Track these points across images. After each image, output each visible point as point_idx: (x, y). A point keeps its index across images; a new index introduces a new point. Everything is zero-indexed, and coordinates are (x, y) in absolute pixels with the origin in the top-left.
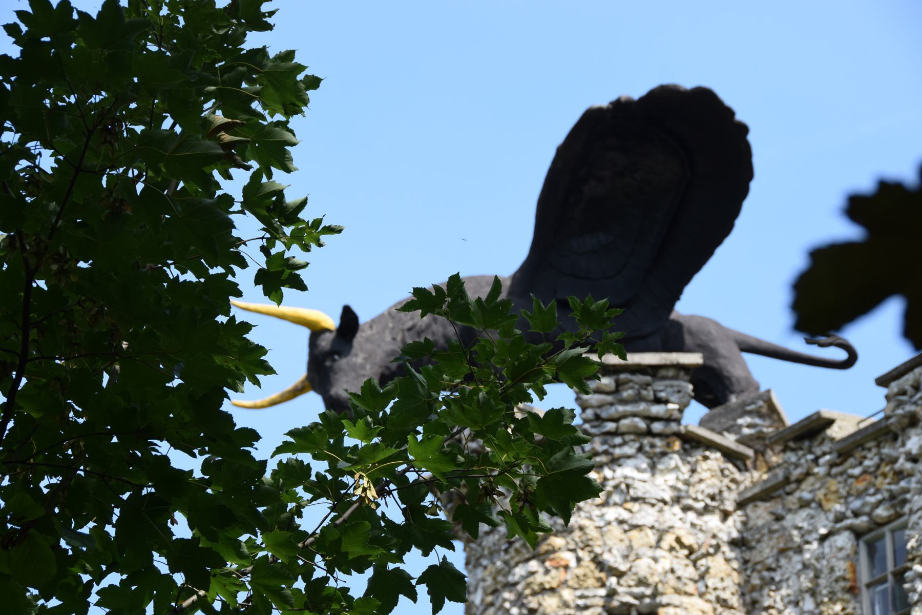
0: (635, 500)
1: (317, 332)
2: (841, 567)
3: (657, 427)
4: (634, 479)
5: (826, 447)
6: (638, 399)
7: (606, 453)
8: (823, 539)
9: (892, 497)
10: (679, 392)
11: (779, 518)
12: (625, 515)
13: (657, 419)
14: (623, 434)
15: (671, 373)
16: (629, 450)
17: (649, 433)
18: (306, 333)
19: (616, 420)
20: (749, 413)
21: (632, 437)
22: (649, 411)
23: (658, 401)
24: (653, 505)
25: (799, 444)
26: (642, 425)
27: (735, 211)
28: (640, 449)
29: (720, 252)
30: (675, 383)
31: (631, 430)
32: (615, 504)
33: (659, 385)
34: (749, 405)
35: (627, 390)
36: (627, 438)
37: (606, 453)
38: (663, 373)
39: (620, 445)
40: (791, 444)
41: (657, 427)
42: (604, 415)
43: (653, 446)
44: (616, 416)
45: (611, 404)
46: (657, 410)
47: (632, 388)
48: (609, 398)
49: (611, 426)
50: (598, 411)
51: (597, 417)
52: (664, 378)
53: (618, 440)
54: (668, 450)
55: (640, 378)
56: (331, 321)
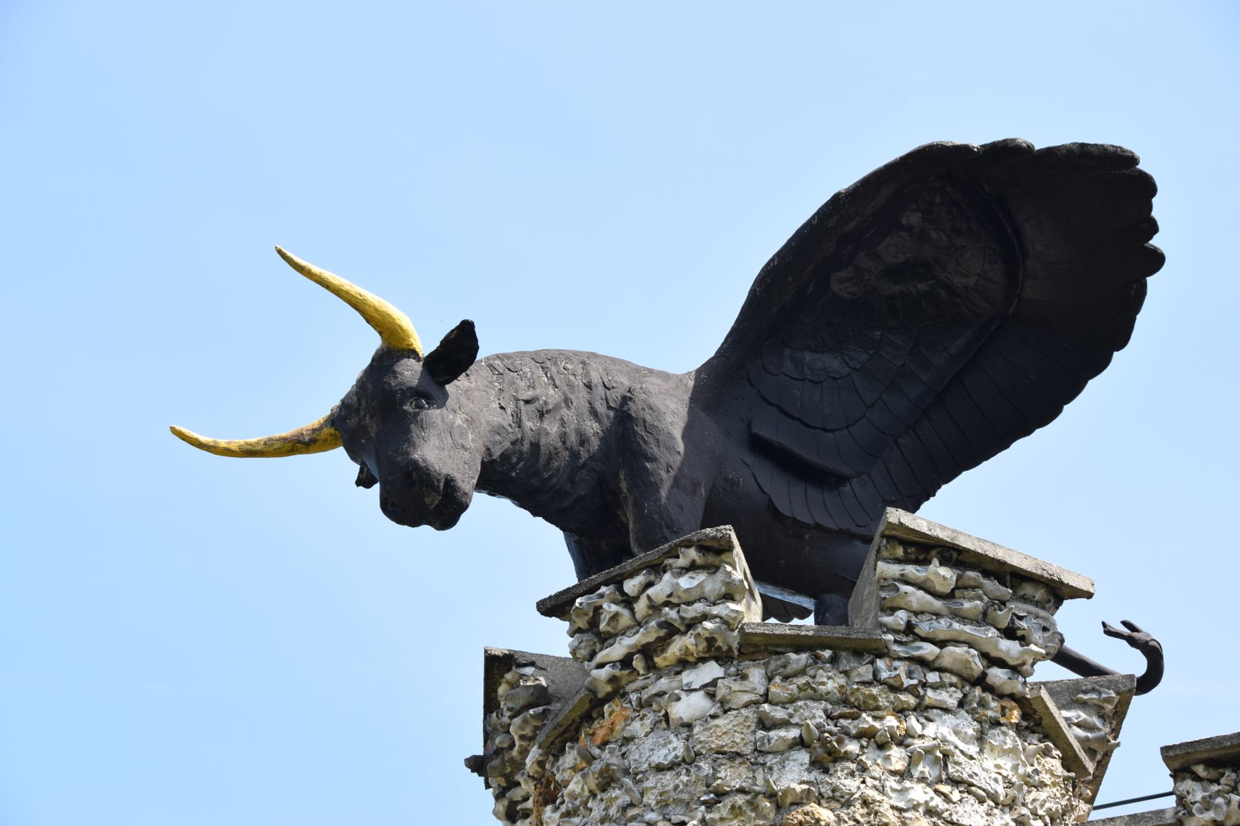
0: (955, 782)
1: (394, 348)
3: (998, 675)
4: (956, 747)
6: (984, 619)
7: (911, 690)
10: (1045, 629)
12: (938, 802)
13: (1001, 663)
14: (941, 670)
15: (1039, 594)
16: (950, 698)
17: (981, 681)
18: (372, 342)
19: (942, 644)
20: (1083, 705)
21: (954, 679)
22: (996, 646)
23: (1009, 633)
24: (981, 801)
25: (1213, 774)
26: (978, 665)
27: (1072, 390)
28: (961, 704)
29: (1019, 445)
30: (1042, 613)
31: (955, 668)
32: (922, 779)
34: (1085, 692)
35: (971, 599)
36: (949, 678)
37: (911, 690)
38: (1028, 590)
39: (935, 687)
40: (1200, 770)
41: (998, 675)
42: (924, 627)
43: (983, 704)
44: (941, 636)
45: (938, 615)
46: (1009, 648)
47: (981, 599)
48: (938, 604)
49: (928, 650)
50: (914, 620)
51: (909, 629)
52: (1024, 599)
53: (933, 677)
54: (1002, 720)
55: (992, 585)
56: (426, 341)
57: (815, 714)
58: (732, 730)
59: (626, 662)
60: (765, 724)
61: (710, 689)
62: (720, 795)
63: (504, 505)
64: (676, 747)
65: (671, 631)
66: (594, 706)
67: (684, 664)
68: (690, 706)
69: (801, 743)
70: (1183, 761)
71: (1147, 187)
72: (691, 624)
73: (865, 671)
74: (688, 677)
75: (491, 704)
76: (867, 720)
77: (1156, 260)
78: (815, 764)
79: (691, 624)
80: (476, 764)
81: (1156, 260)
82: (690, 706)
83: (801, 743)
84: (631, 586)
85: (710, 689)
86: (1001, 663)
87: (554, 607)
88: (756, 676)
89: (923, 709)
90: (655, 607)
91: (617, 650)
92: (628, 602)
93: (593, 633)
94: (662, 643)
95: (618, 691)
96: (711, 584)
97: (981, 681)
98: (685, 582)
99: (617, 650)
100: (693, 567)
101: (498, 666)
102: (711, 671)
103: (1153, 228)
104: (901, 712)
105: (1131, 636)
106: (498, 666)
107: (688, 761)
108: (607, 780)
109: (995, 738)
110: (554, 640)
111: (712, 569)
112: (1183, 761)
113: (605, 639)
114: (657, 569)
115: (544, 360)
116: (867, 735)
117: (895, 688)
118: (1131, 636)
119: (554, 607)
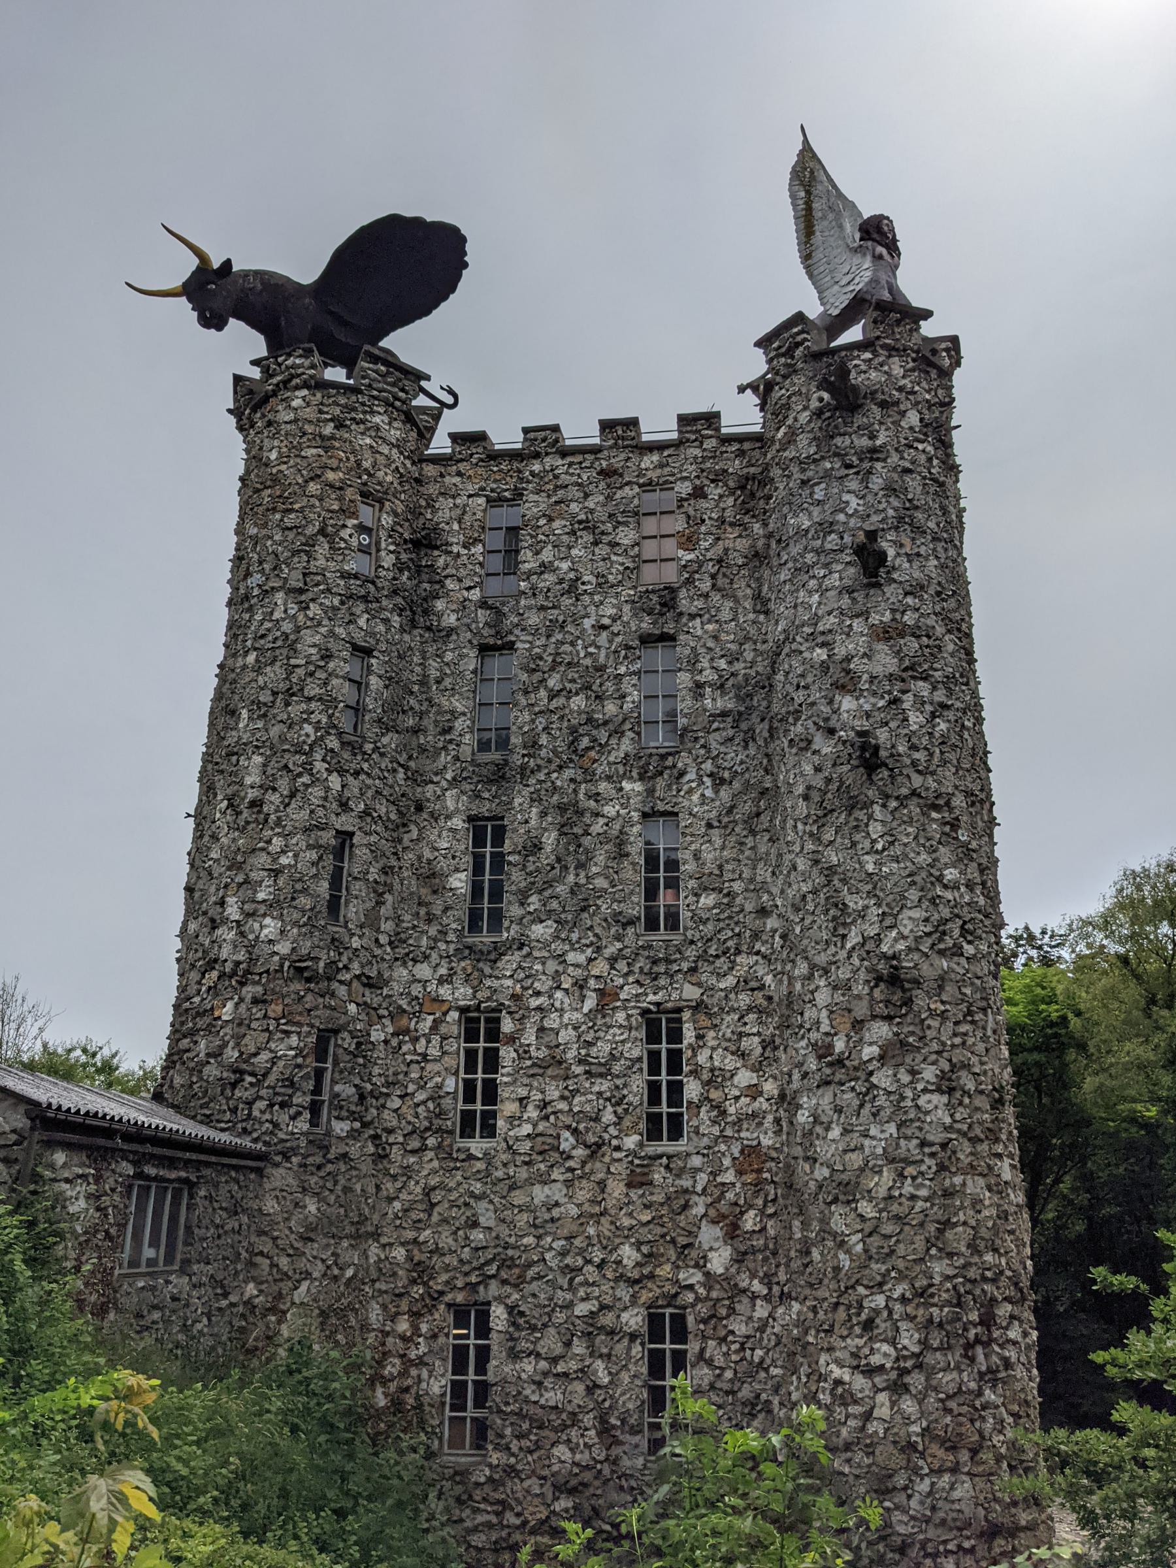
2: (479, 515)
3: (398, 404)
5: (480, 450)
6: (394, 385)
8: (470, 496)
9: (516, 489)
11: (442, 476)
13: (399, 399)
16: (381, 410)
17: (392, 405)
18: (195, 262)
23: (403, 390)
29: (418, 322)
33: (406, 382)
41: (398, 404)
46: (401, 394)
49: (375, 393)
51: (370, 385)
57: (337, 411)
58: (310, 413)
59: (277, 385)
60: (321, 412)
61: (304, 398)
62: (305, 434)
63: (242, 324)
64: (292, 416)
65: (292, 377)
66: (266, 399)
67: (297, 388)
68: (296, 403)
69: (331, 420)
70: (455, 437)
71: (464, 240)
72: (299, 376)
73: (354, 398)
74: (297, 393)
75: (235, 392)
76: (353, 415)
77: (466, 265)
78: (336, 427)
79: (299, 376)
80: (229, 411)
81: (466, 265)
82: (296, 403)
83: (331, 420)
84: (280, 359)
85: (304, 398)
86: (399, 399)
87: (255, 363)
88: (319, 395)
89: (372, 412)
90: (287, 368)
91: (275, 381)
92: (280, 365)
93: (267, 373)
94: (290, 380)
95: (274, 394)
96: (307, 363)
97: (392, 405)
98: (298, 361)
99: (275, 381)
100: (300, 356)
101: (238, 379)
102: (305, 392)
103: (465, 254)
104: (365, 412)
105: (451, 392)
106: (238, 379)
107: (296, 421)
108: (270, 424)
109: (395, 424)
110: (255, 373)
111: (307, 357)
112: (455, 437)
113: (272, 376)
114: (289, 355)
115: (257, 273)
116: (353, 419)
117: (363, 404)
118: (451, 392)
119: (255, 363)
